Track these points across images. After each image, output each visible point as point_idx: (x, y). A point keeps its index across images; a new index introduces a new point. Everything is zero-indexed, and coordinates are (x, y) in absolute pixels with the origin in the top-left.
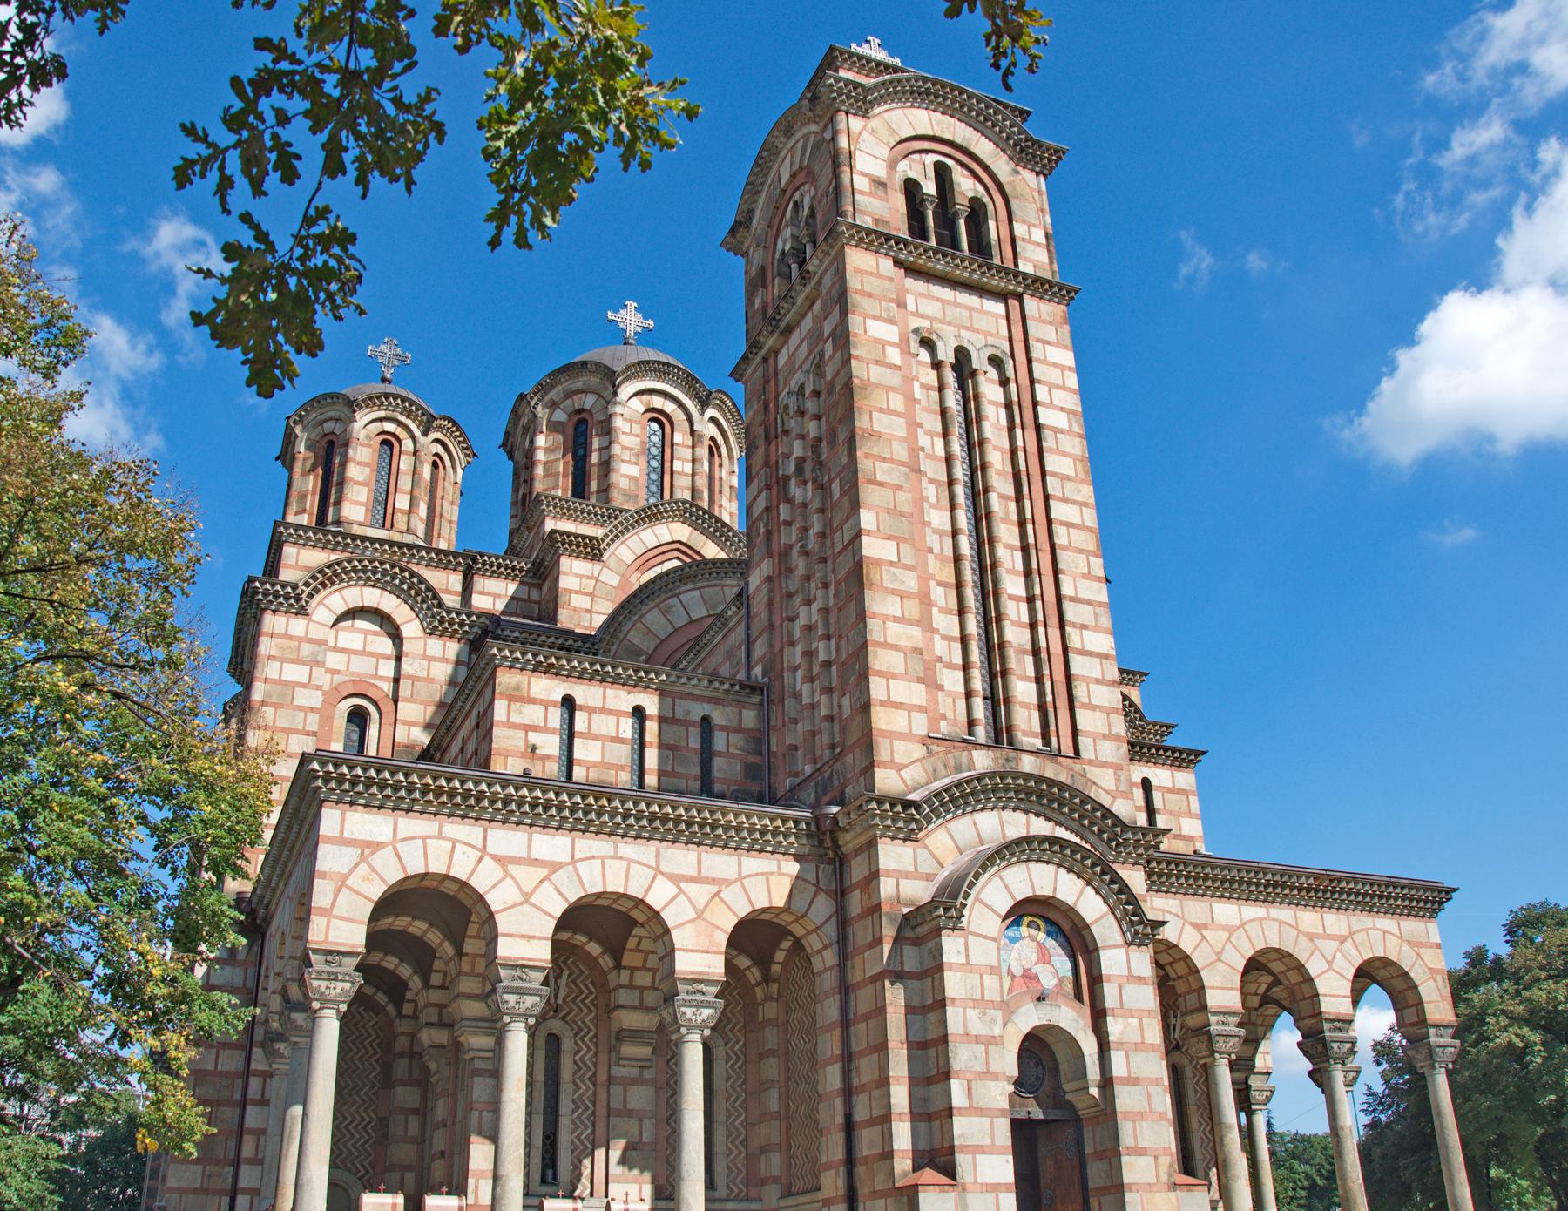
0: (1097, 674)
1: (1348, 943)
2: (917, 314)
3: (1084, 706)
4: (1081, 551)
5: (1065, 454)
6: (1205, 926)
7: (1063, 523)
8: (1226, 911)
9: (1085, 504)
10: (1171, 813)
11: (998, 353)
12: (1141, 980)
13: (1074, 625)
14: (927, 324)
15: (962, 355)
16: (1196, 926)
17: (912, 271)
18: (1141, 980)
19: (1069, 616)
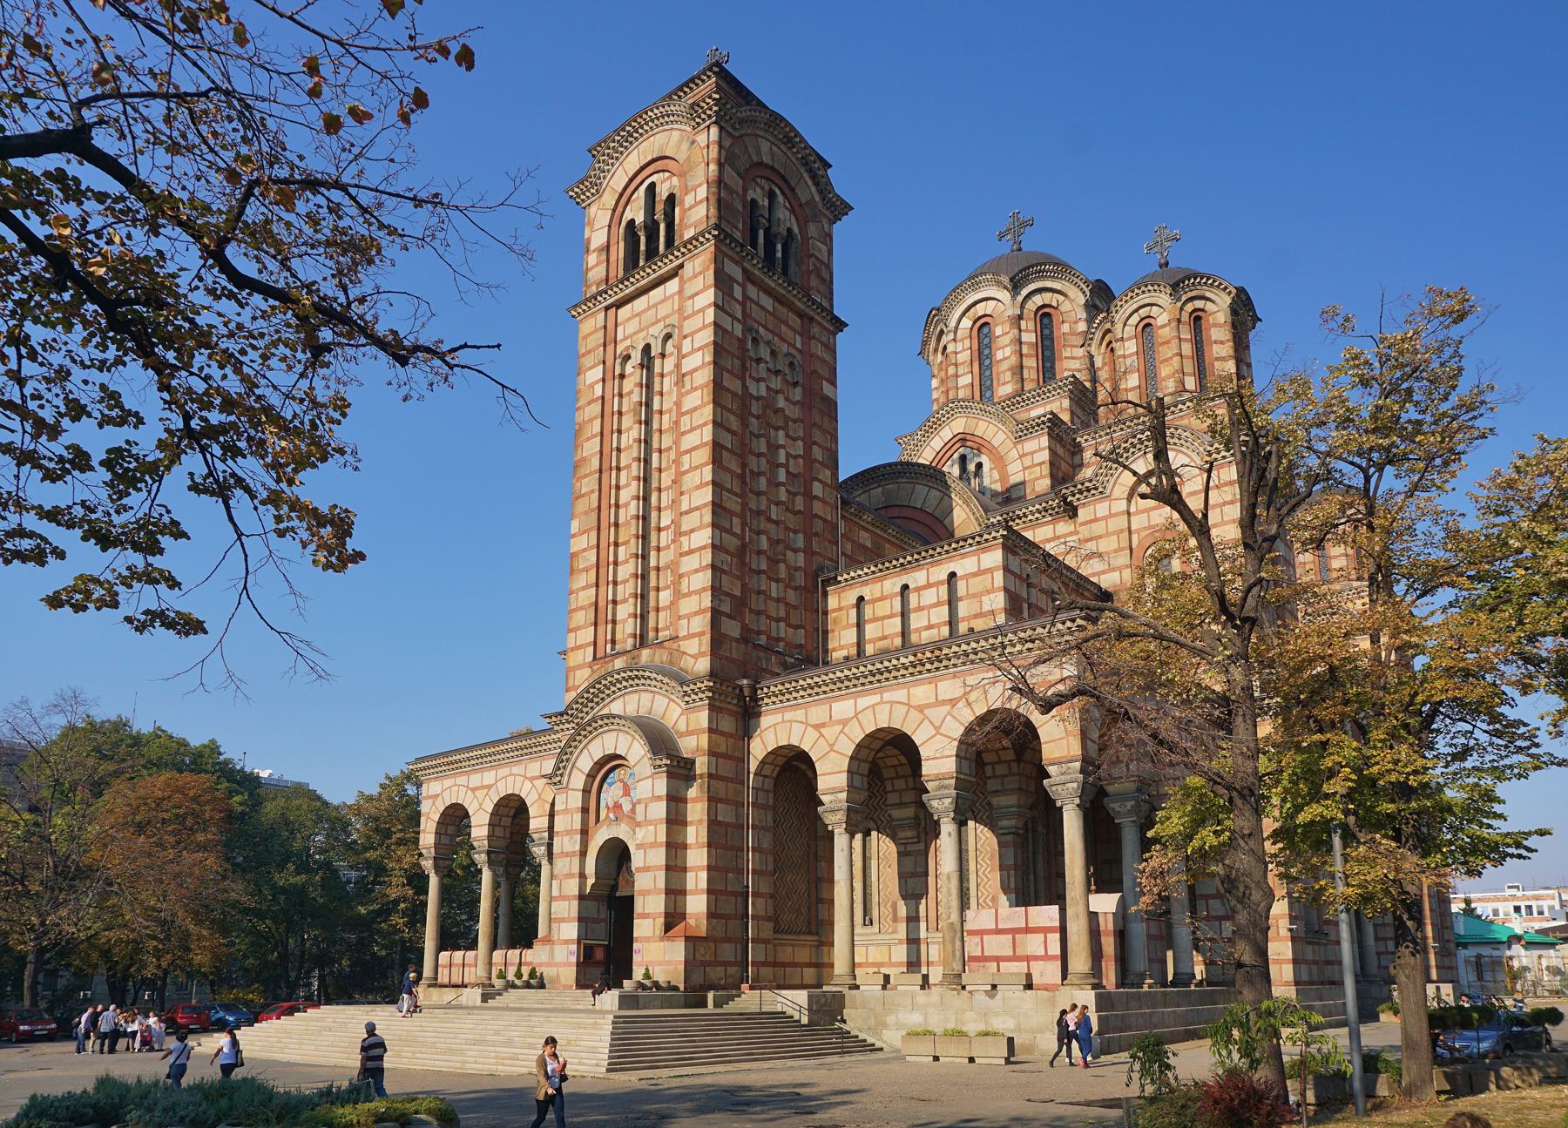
0: (697, 566)
1: (960, 705)
2: (626, 338)
3: (685, 596)
4: (696, 468)
5: (696, 389)
6: (823, 725)
7: (687, 452)
8: (843, 708)
9: (705, 424)
10: (974, 596)
11: (668, 330)
12: (659, 798)
13: (685, 533)
14: (628, 342)
15: (647, 349)
16: (817, 727)
17: (619, 305)
18: (659, 798)
19: (684, 528)
